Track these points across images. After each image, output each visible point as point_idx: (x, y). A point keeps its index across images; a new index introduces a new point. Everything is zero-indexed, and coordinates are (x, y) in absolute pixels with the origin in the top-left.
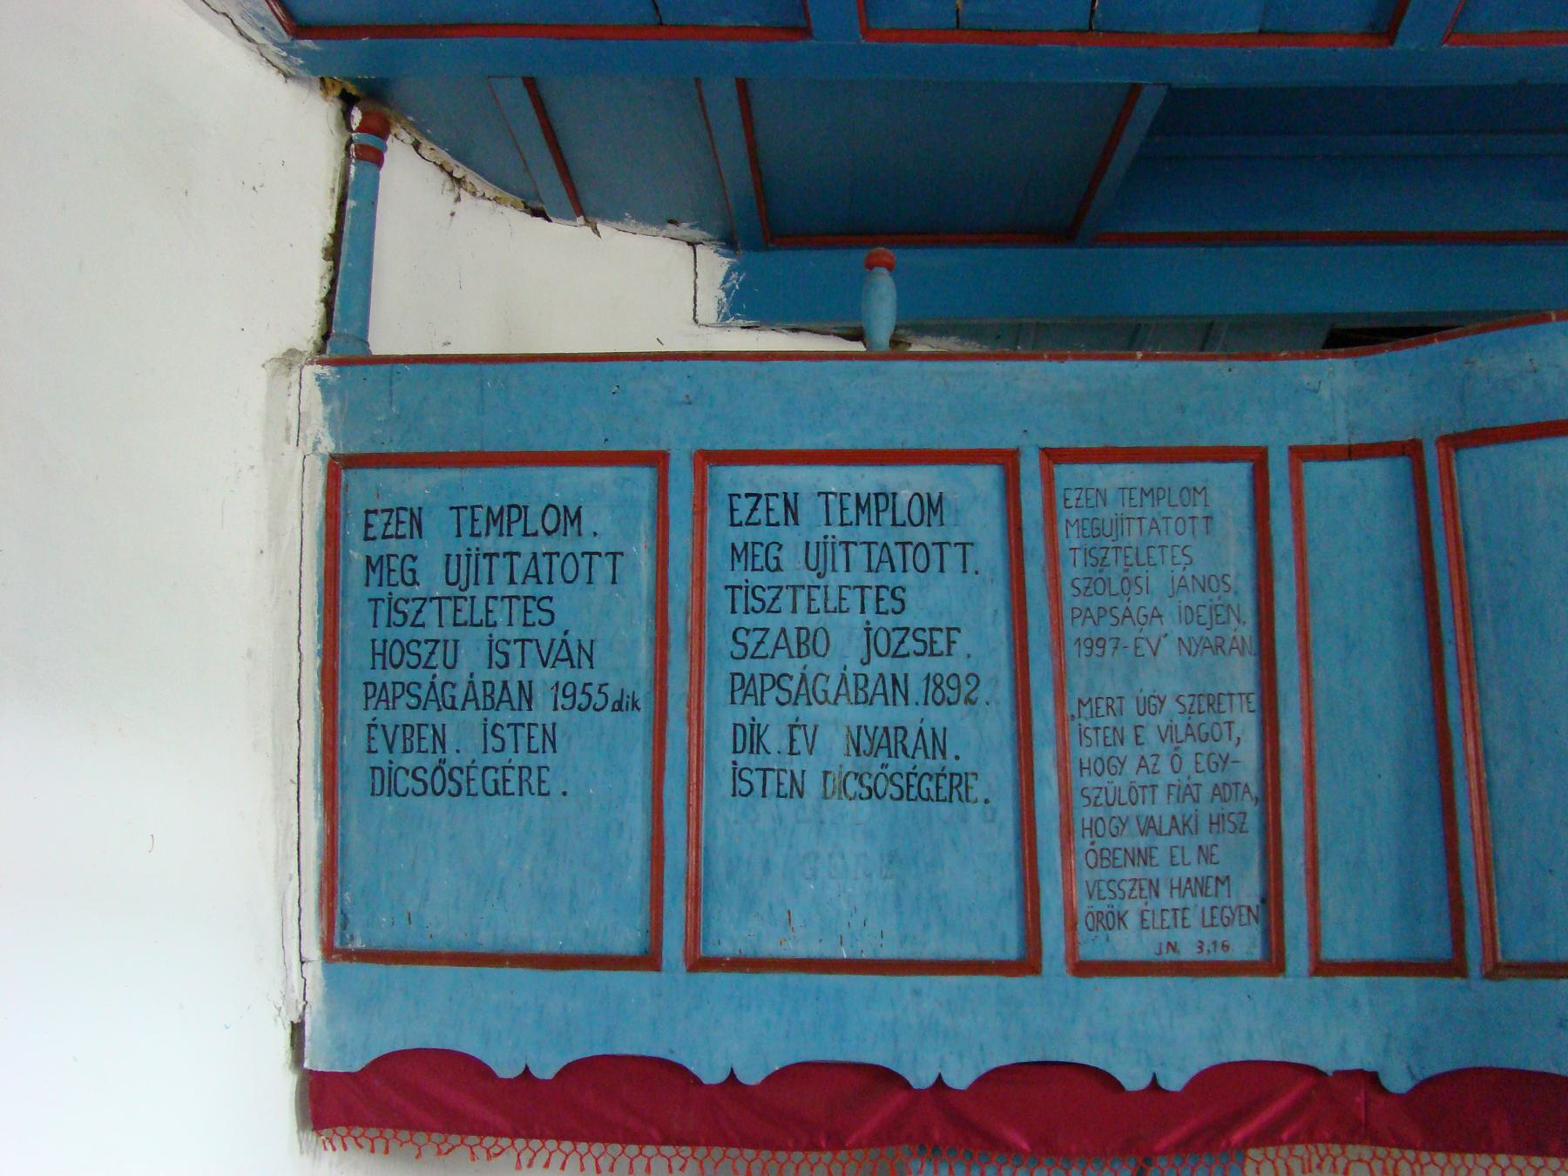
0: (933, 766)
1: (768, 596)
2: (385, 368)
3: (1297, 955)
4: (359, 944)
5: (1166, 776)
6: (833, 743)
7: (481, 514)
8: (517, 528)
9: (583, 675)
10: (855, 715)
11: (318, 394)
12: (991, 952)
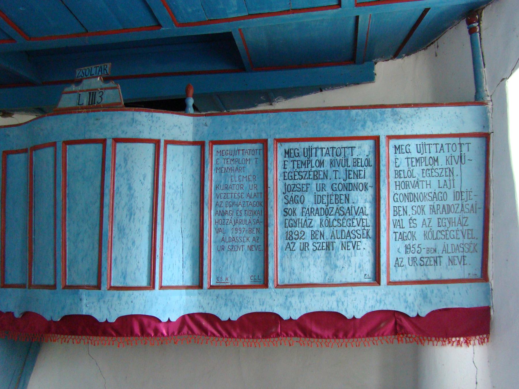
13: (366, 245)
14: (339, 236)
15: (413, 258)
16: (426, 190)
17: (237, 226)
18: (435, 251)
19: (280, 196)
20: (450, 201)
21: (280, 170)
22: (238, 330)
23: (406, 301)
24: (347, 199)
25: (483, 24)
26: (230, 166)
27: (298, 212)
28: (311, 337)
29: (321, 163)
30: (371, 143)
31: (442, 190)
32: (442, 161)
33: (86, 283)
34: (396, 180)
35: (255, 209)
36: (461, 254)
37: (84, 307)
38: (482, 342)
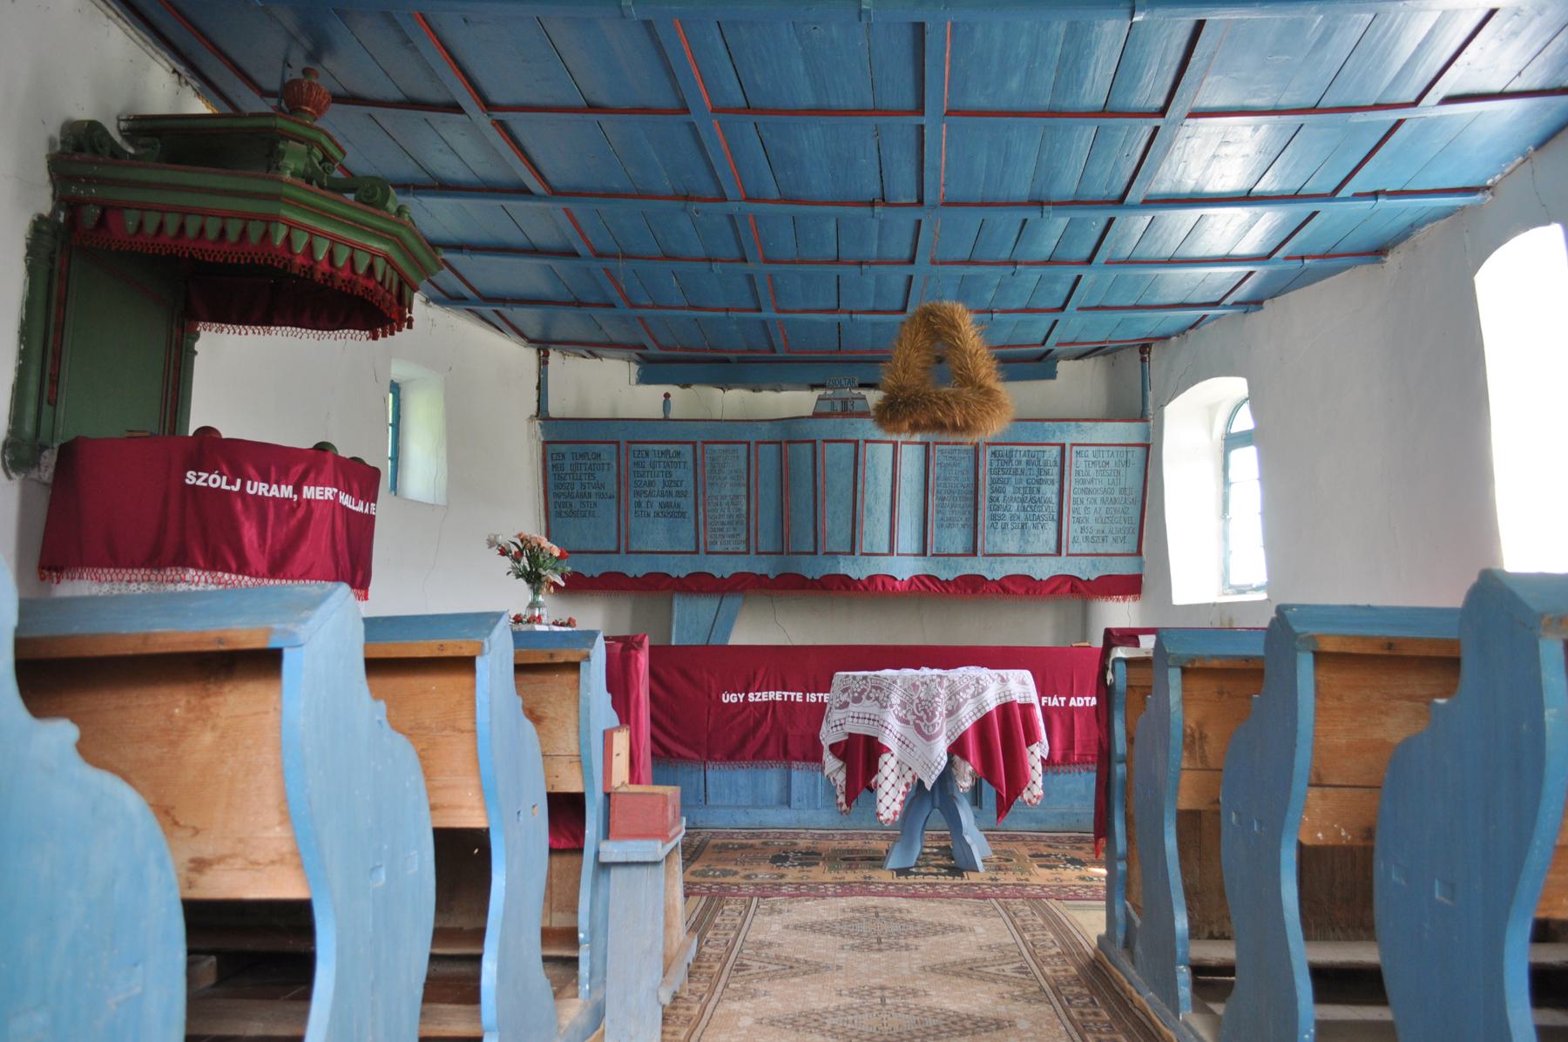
2: (554, 422)
3: (753, 551)
6: (656, 505)
10: (661, 499)
11: (539, 427)
12: (690, 550)
13: (1052, 526)
15: (1086, 537)
16: (1098, 486)
19: (988, 486)
20: (1116, 495)
21: (988, 467)
22: (953, 588)
23: (1080, 568)
24: (1039, 491)
27: (1001, 499)
28: (1008, 593)
29: (1019, 462)
30: (1058, 448)
32: (1112, 464)
33: (842, 551)
37: (842, 569)
38: (1135, 600)
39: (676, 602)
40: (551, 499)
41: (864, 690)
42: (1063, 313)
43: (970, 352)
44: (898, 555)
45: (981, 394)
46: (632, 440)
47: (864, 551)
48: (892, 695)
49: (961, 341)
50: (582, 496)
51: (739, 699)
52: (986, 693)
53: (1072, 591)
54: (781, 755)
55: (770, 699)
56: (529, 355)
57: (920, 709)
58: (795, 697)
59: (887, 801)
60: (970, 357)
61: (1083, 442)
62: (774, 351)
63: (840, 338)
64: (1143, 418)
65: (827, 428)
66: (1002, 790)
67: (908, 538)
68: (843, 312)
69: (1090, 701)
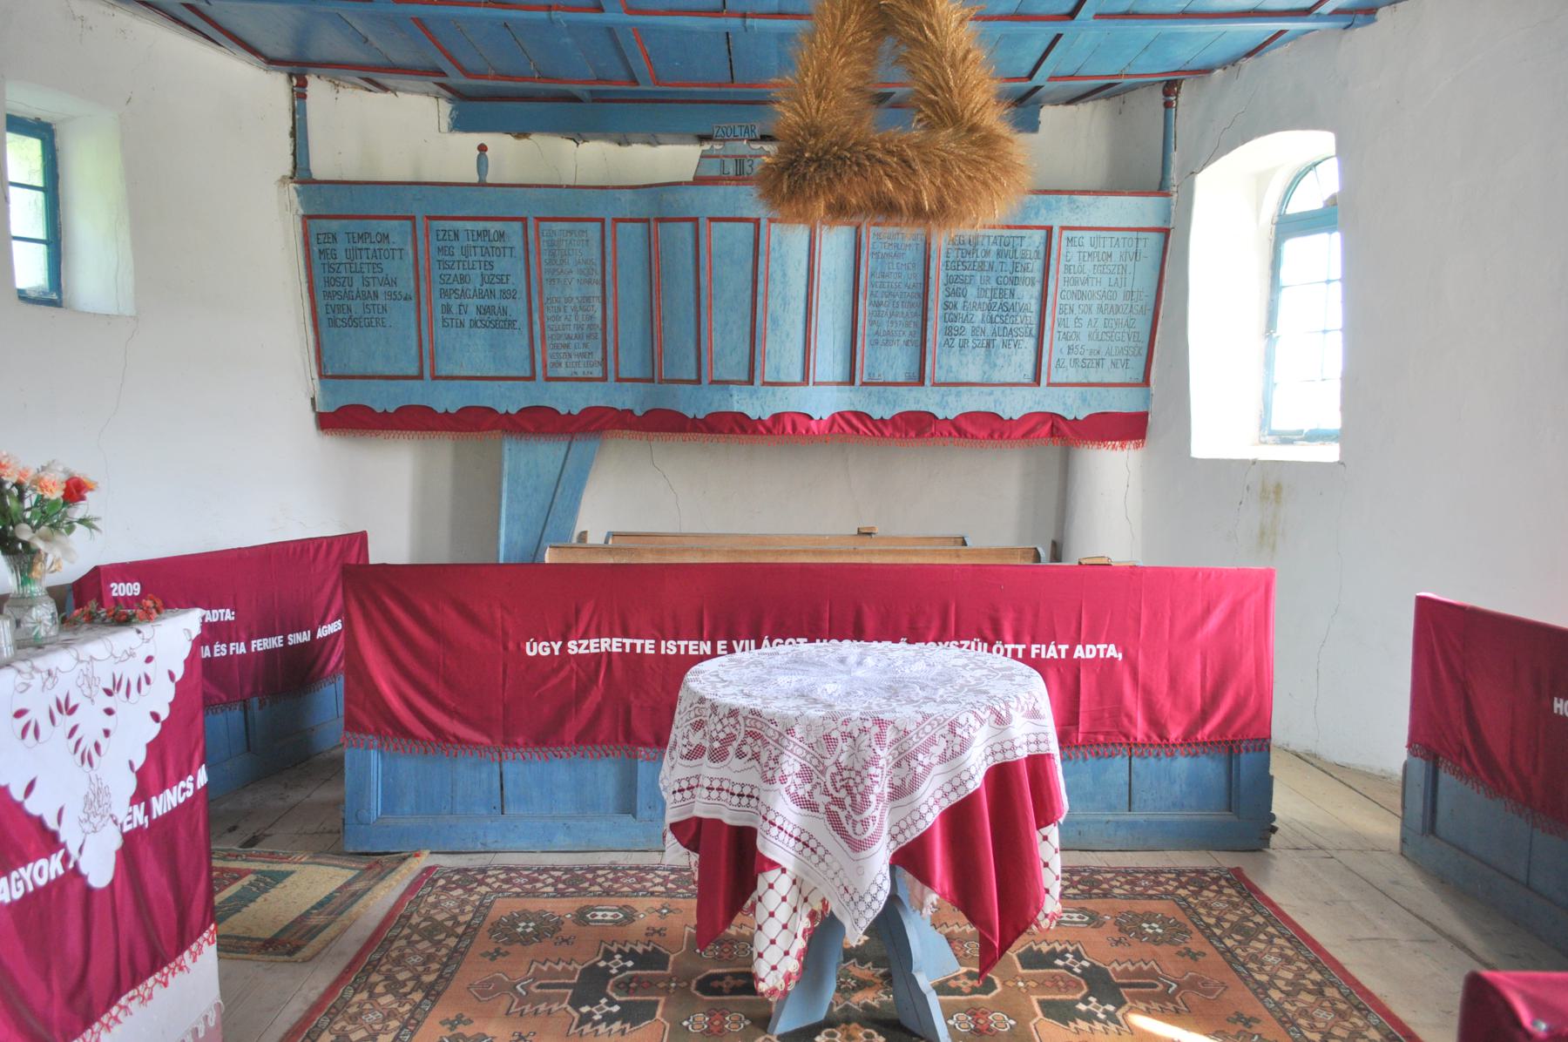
0: (503, 318)
1: (450, 264)
2: (317, 185)
3: (611, 376)
4: (330, 373)
5: (574, 322)
6: (472, 310)
7: (356, 235)
8: (368, 240)
9: (394, 289)
11: (295, 194)
12: (522, 374)
13: (1029, 344)
14: (1001, 333)
16: (1095, 289)
17: (893, 318)
18: (1098, 352)
19: (942, 288)
20: (1119, 301)
21: (943, 259)
23: (1065, 404)
24: (1012, 294)
25: (1182, 98)
26: (888, 251)
27: (959, 306)
28: (966, 437)
29: (987, 253)
30: (1043, 233)
31: (1111, 288)
32: (1116, 257)
33: (735, 378)
34: (1065, 275)
35: (914, 300)
36: (1125, 357)
39: (506, 447)
40: (321, 302)
41: (731, 737)
42: (1074, 22)
43: (953, 53)
44: (814, 383)
45: (973, 143)
46: (433, 214)
47: (767, 379)
48: (784, 758)
49: (934, 33)
50: (364, 296)
51: (552, 650)
52: (968, 753)
53: (1052, 435)
54: (621, 738)
55: (603, 650)
56: (276, 85)
57: (838, 785)
58: (643, 646)
59: (772, 955)
60: (953, 66)
61: (1077, 225)
62: (635, 82)
63: (731, 61)
64: (1162, 190)
65: (715, 199)
66: (992, 934)
67: (828, 361)
68: (732, 14)
69: (1106, 650)
